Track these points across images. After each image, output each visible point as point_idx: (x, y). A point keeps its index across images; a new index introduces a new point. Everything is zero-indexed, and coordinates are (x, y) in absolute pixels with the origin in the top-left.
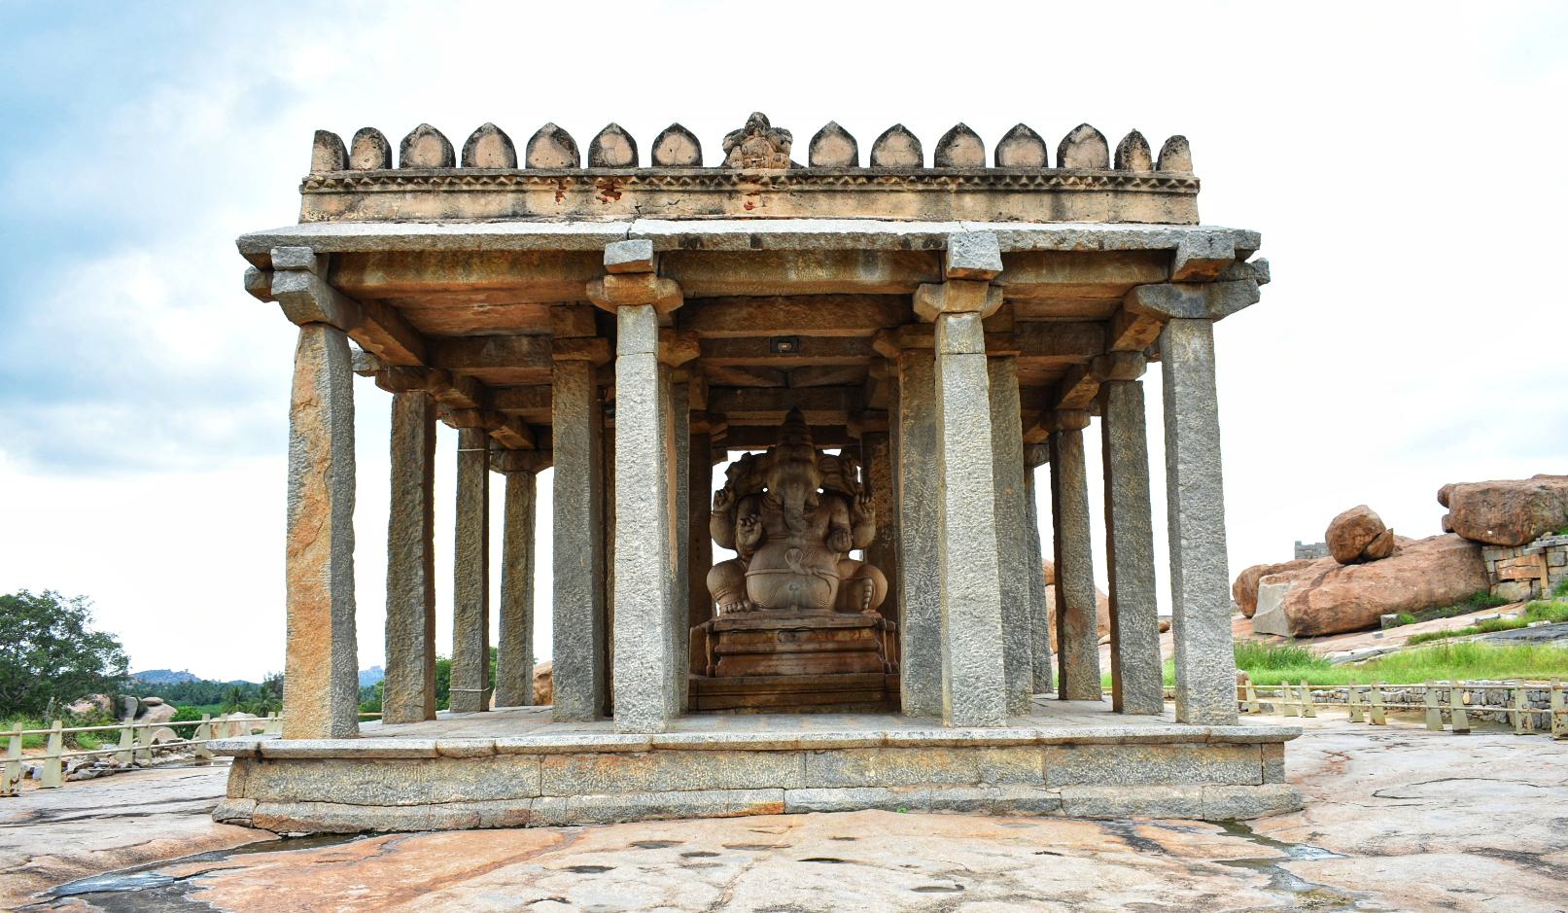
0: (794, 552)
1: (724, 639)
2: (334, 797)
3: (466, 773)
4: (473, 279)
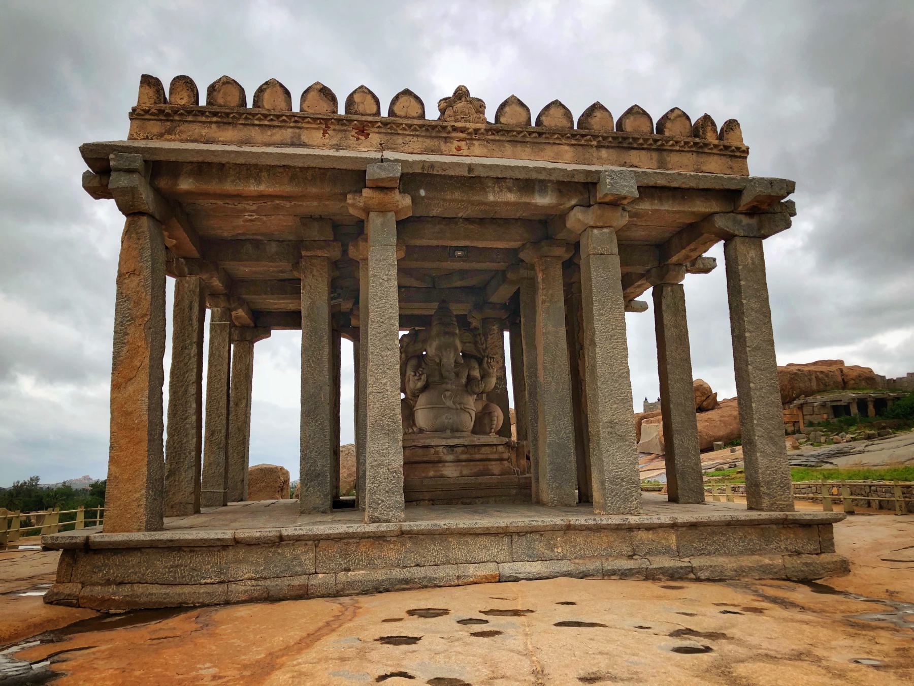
0: (448, 394)
2: (149, 579)
3: (257, 556)
4: (262, 188)
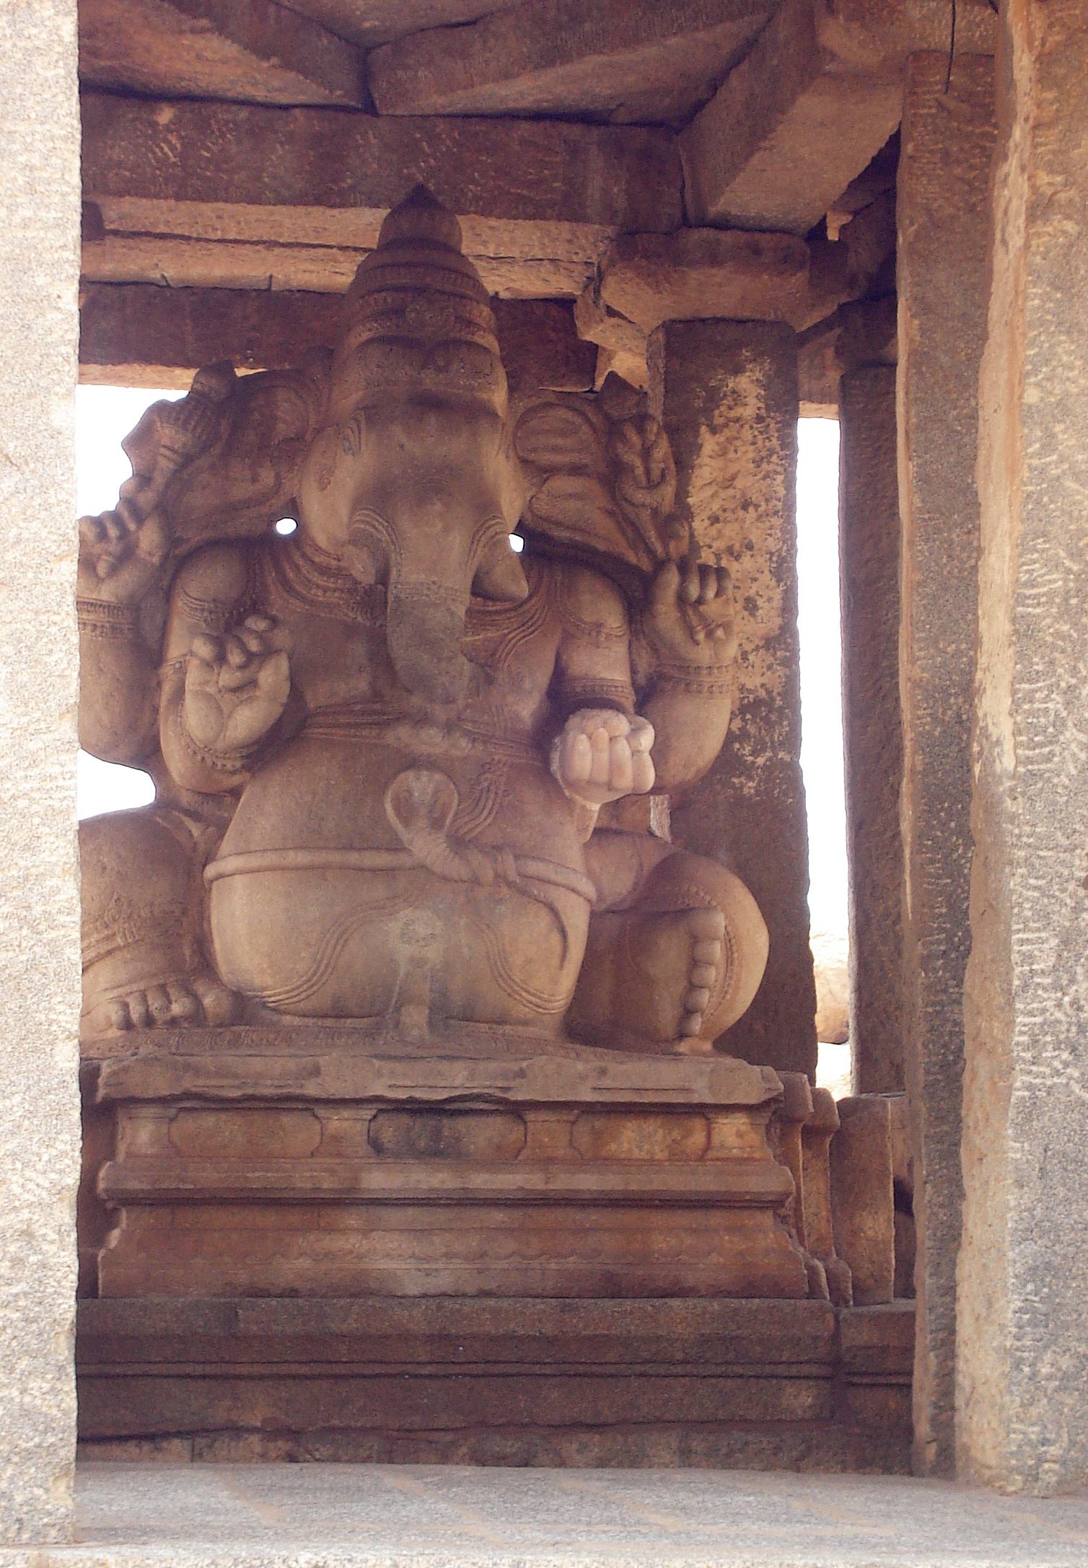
0: (421, 785)
1: (141, 1134)
